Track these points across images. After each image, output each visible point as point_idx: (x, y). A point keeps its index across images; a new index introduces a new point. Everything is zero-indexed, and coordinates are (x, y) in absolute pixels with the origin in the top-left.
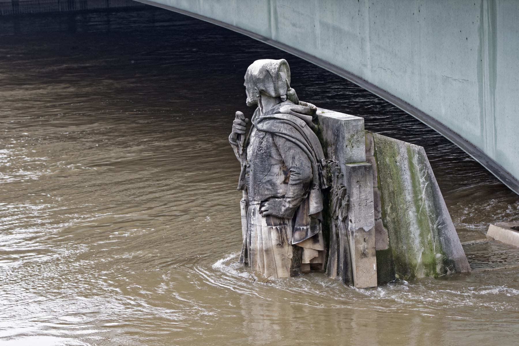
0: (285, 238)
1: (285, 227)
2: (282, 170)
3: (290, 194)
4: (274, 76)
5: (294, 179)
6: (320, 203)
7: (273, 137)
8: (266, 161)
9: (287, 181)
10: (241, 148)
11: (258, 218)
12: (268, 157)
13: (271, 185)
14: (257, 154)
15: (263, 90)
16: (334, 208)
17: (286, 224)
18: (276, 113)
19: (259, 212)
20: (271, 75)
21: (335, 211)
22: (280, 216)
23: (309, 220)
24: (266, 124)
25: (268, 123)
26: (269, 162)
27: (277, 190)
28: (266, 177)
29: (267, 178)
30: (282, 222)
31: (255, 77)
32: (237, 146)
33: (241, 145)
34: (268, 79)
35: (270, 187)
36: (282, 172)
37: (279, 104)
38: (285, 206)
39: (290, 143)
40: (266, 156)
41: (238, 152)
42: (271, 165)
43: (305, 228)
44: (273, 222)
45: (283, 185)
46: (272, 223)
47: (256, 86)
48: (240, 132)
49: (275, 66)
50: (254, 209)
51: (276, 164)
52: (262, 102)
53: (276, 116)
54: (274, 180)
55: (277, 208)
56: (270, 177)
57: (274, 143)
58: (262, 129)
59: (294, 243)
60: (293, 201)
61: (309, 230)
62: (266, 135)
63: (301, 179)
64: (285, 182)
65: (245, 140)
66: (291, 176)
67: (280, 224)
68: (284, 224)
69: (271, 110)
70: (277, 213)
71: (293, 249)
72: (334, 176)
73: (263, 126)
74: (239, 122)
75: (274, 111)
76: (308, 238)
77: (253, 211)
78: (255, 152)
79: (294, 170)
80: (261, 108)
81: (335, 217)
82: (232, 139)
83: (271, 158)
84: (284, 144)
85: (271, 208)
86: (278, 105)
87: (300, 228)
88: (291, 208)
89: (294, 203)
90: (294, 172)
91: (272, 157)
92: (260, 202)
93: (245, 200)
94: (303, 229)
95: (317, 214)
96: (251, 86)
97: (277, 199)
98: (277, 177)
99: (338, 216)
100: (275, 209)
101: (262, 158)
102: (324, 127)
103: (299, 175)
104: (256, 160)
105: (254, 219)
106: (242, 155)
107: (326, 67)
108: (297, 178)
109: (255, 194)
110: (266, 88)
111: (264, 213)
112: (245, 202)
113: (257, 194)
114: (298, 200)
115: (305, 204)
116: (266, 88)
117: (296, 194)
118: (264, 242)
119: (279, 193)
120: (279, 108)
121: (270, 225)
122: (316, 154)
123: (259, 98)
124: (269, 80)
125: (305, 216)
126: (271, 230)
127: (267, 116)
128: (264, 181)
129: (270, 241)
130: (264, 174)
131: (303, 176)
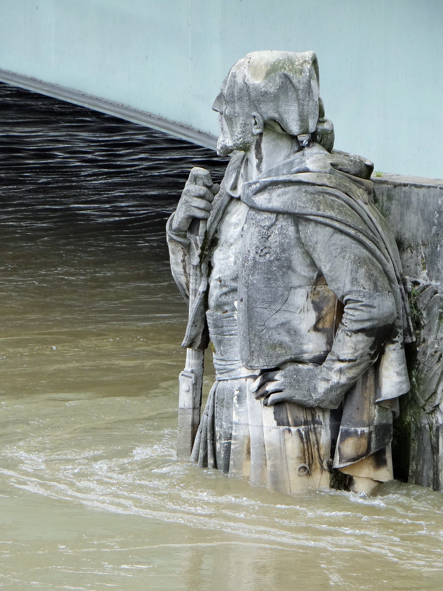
0: (316, 454)
1: (315, 429)
2: (310, 300)
3: (346, 351)
4: (301, 87)
5: (359, 318)
6: (405, 375)
7: (296, 225)
8: (280, 278)
9: (320, 326)
10: (197, 252)
11: (252, 409)
12: (284, 270)
13: (288, 332)
14: (255, 262)
15: (274, 120)
16: (434, 387)
17: (320, 423)
18: (298, 172)
19: (254, 396)
20: (294, 86)
21: (435, 393)
22: (312, 402)
23: (375, 412)
24: (279, 196)
25: (284, 194)
26: (286, 280)
27: (301, 344)
28: (277, 316)
29: (280, 318)
30: (310, 418)
31: (256, 88)
32: (187, 248)
33: (197, 245)
34: (286, 93)
35: (286, 339)
36: (311, 305)
37: (300, 153)
38: (328, 380)
39: (343, 237)
40: (280, 267)
41: (183, 261)
42: (290, 288)
43: (366, 430)
44: (292, 417)
45: (313, 334)
46: (290, 420)
47: (256, 109)
48: (200, 214)
49: (302, 65)
50: (240, 389)
51: (300, 286)
52: (263, 145)
53: (302, 177)
54: (295, 323)
55: (305, 385)
56: (287, 316)
57: (299, 239)
58: (270, 206)
59: (342, 466)
60: (350, 368)
61: (373, 435)
62: (277, 220)
63: (376, 319)
64: (316, 328)
65: (206, 233)
66: (350, 312)
67: (306, 423)
68: (314, 422)
69: (284, 165)
70: (305, 397)
71: (332, 479)
72: (428, 314)
73: (270, 200)
74: (202, 193)
75: (292, 167)
76: (371, 453)
77: (236, 393)
78: (251, 258)
79: (360, 299)
80: (254, 161)
81: (429, 408)
82: (175, 231)
83: (290, 272)
84: (329, 240)
85: (291, 385)
86: (299, 154)
87: (356, 432)
88: (344, 385)
89: (351, 373)
90: (358, 301)
91: (294, 271)
92: (257, 373)
93: (192, 372)
94: (363, 432)
95: (392, 401)
96: (242, 108)
97: (300, 366)
98: (302, 316)
99: (438, 406)
100: (300, 388)
101: (269, 272)
102: (393, 207)
103: (372, 310)
104: (253, 275)
105: (241, 410)
106: (195, 267)
107: (85, 103)
108: (365, 316)
109: (252, 353)
110: (280, 115)
111: (272, 397)
112: (193, 375)
113: (256, 354)
114: (363, 365)
115: (367, 379)
116: (280, 115)
117: (360, 352)
118: (269, 463)
119: (306, 353)
120: (302, 162)
121: (284, 425)
122: (395, 264)
123: (258, 137)
124: (287, 97)
125: (367, 402)
126: (287, 435)
127: (281, 178)
128: (272, 324)
129: (284, 461)
130: (273, 307)
131: (381, 312)
